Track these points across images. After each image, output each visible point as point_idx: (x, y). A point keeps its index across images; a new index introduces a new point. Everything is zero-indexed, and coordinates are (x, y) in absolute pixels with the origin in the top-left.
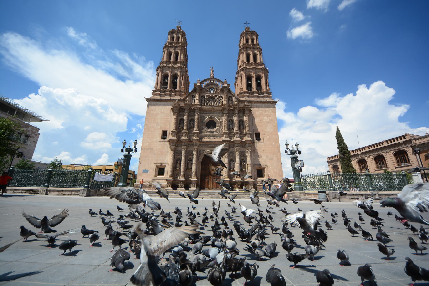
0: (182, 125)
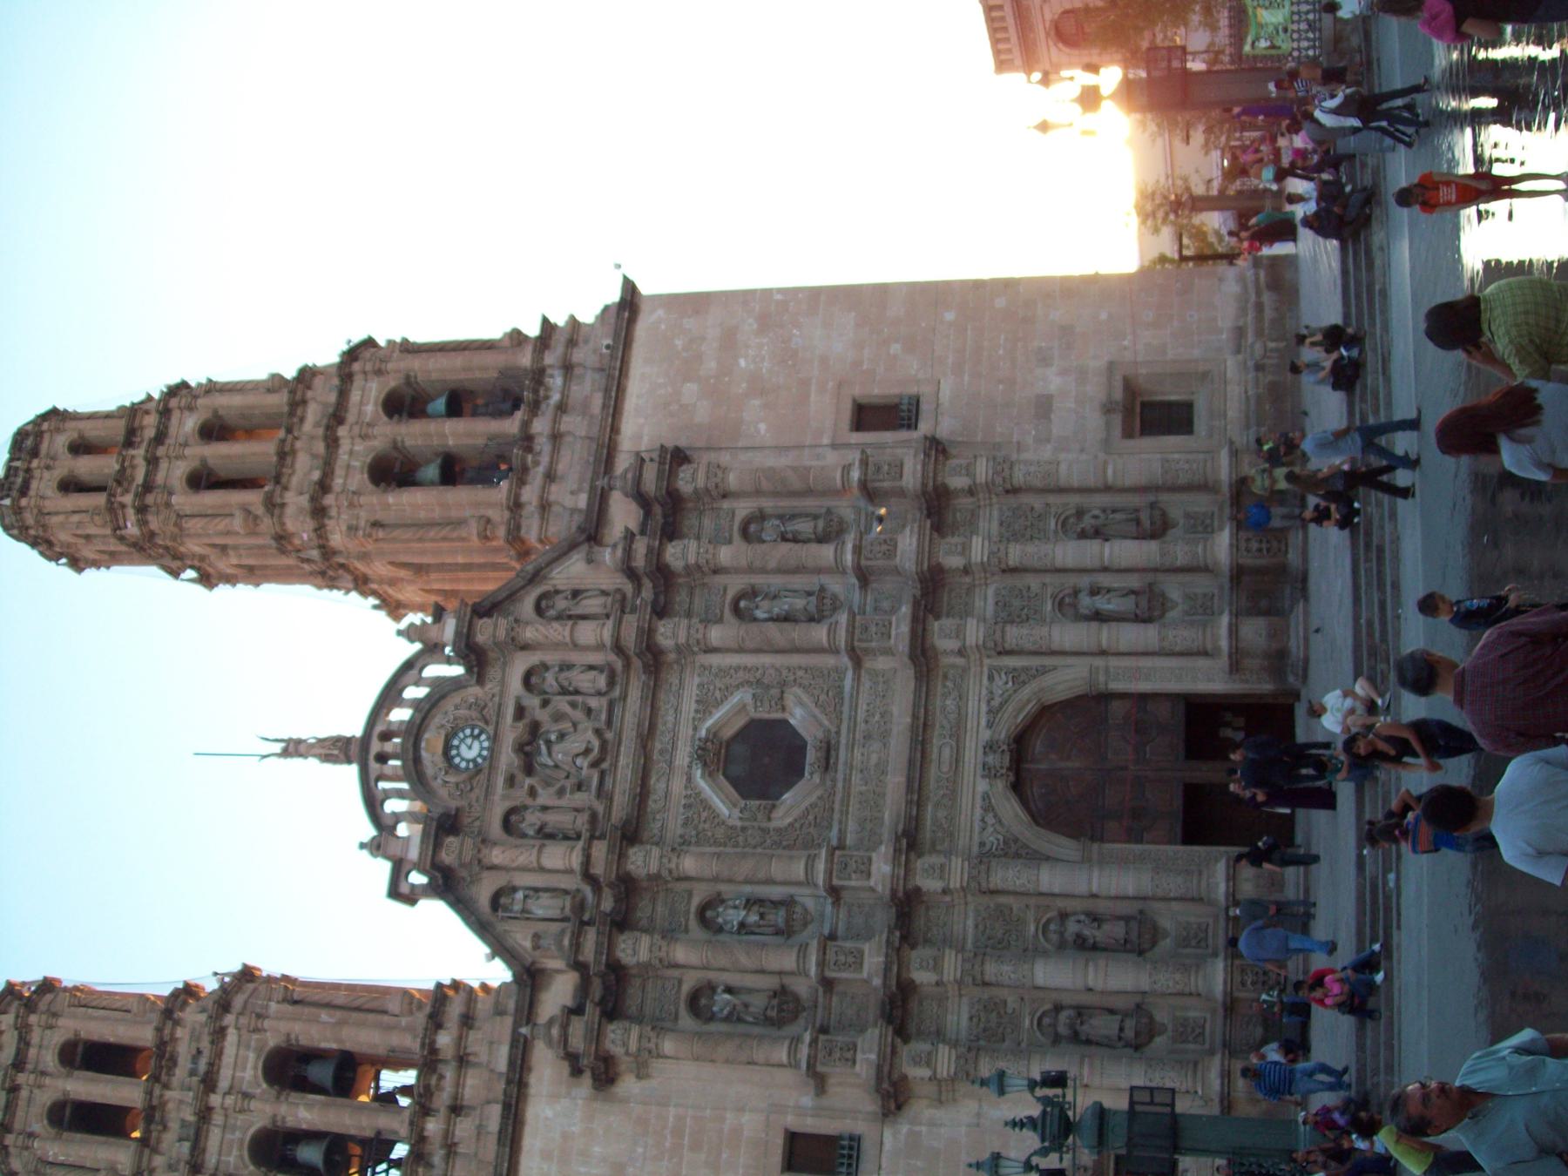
0: (745, 998)
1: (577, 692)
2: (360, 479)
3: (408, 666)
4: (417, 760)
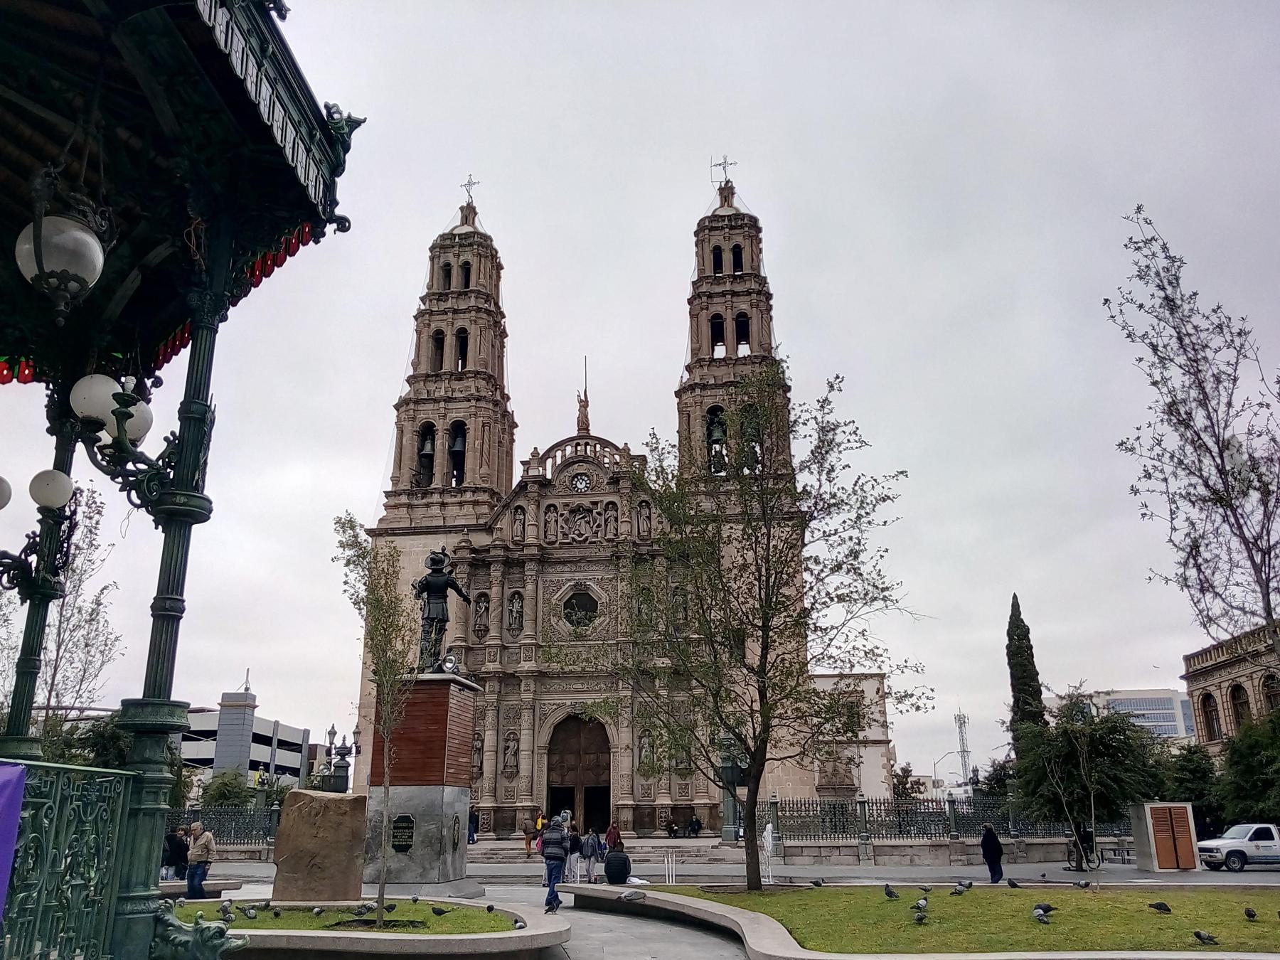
1: (606, 526)
2: (709, 402)
3: (616, 448)
4: (575, 463)
